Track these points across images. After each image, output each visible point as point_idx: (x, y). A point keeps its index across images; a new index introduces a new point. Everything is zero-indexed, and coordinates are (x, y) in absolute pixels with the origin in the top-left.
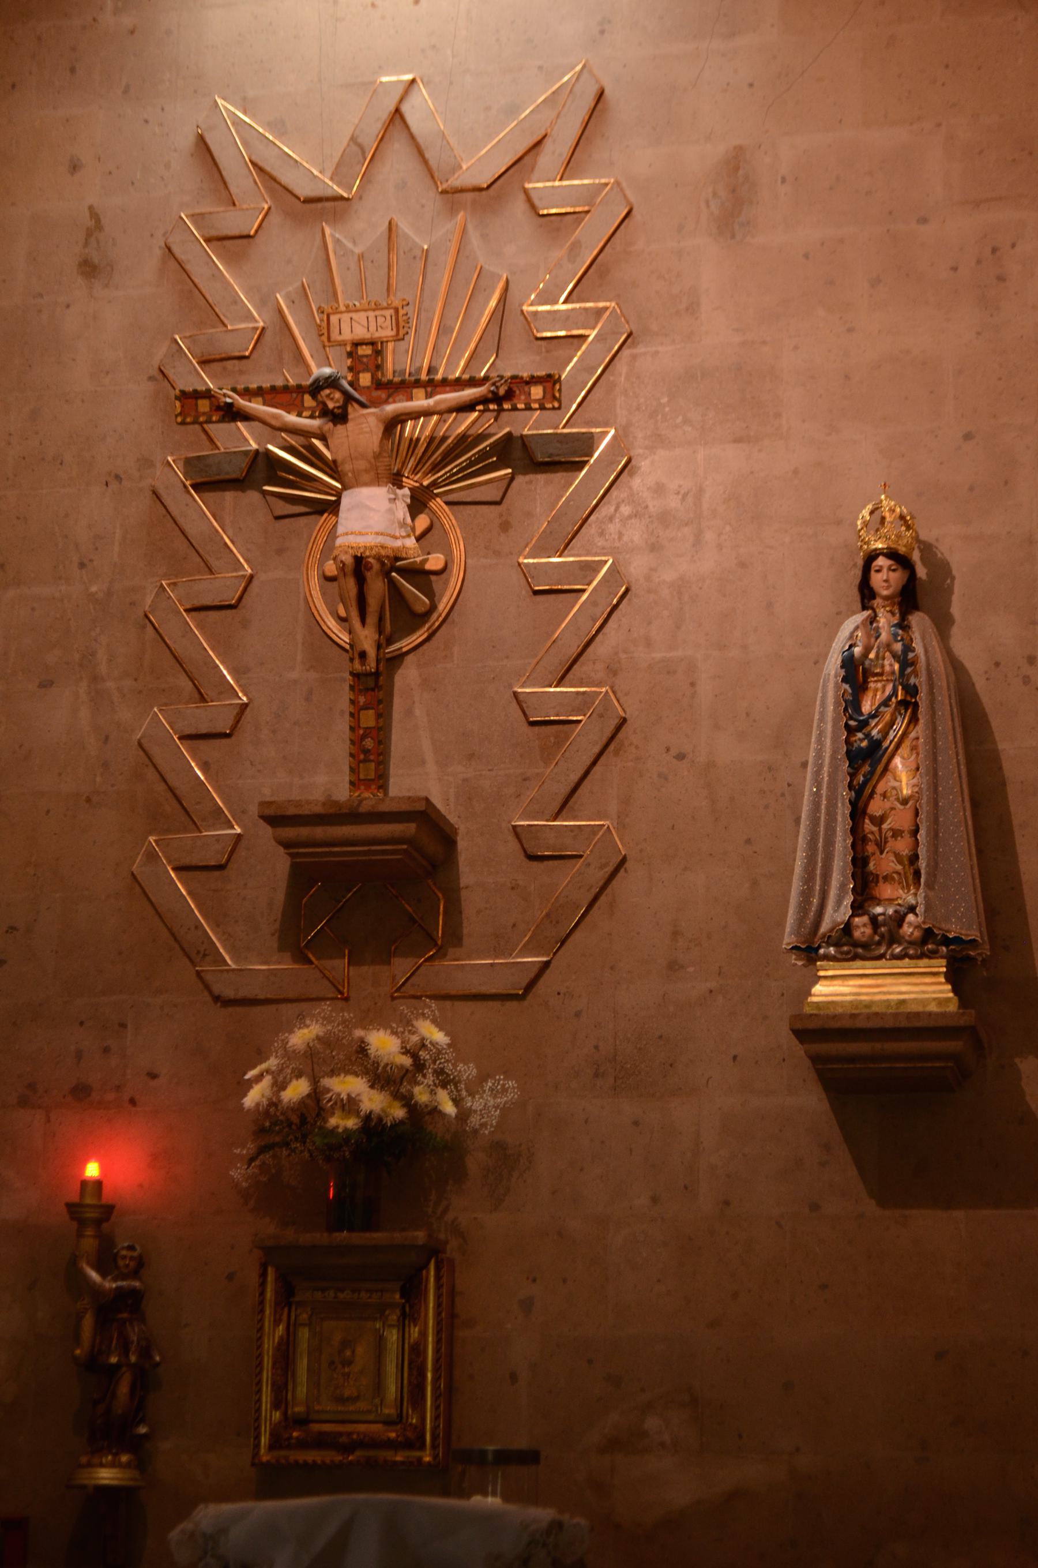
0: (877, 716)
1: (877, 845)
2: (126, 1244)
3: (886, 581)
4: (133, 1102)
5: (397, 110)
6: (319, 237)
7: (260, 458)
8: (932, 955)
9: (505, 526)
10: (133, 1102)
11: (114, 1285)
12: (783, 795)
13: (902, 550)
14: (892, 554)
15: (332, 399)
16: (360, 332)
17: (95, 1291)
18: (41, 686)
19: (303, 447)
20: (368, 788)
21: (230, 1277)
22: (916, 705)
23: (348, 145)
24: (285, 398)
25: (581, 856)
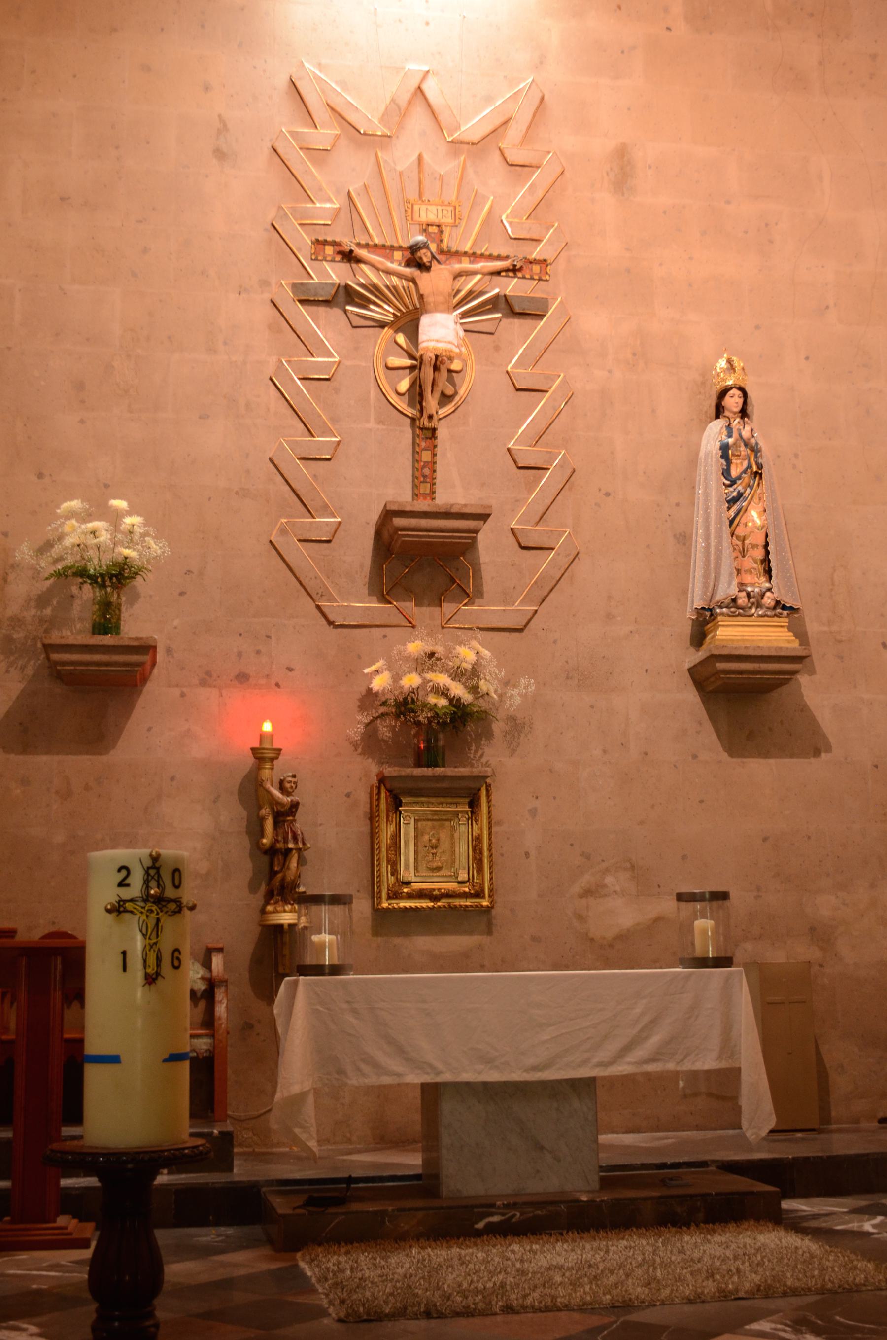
0: (740, 479)
1: (740, 552)
2: (290, 774)
3: (737, 403)
4: (277, 685)
5: (419, 87)
6: (373, 158)
7: (340, 289)
8: (779, 616)
9: (497, 348)
10: (277, 685)
11: (289, 799)
12: (666, 521)
13: (742, 385)
14: (742, 390)
15: (426, 256)
16: (432, 218)
17: (273, 802)
18: (200, 417)
19: (371, 285)
20: (425, 499)
21: (348, 795)
22: (761, 474)
23: (390, 103)
24: (382, 251)
25: (553, 549)
